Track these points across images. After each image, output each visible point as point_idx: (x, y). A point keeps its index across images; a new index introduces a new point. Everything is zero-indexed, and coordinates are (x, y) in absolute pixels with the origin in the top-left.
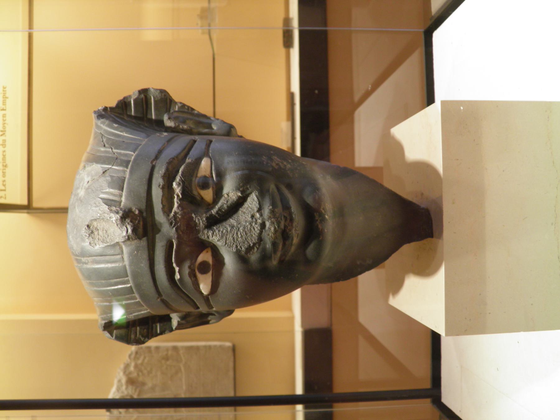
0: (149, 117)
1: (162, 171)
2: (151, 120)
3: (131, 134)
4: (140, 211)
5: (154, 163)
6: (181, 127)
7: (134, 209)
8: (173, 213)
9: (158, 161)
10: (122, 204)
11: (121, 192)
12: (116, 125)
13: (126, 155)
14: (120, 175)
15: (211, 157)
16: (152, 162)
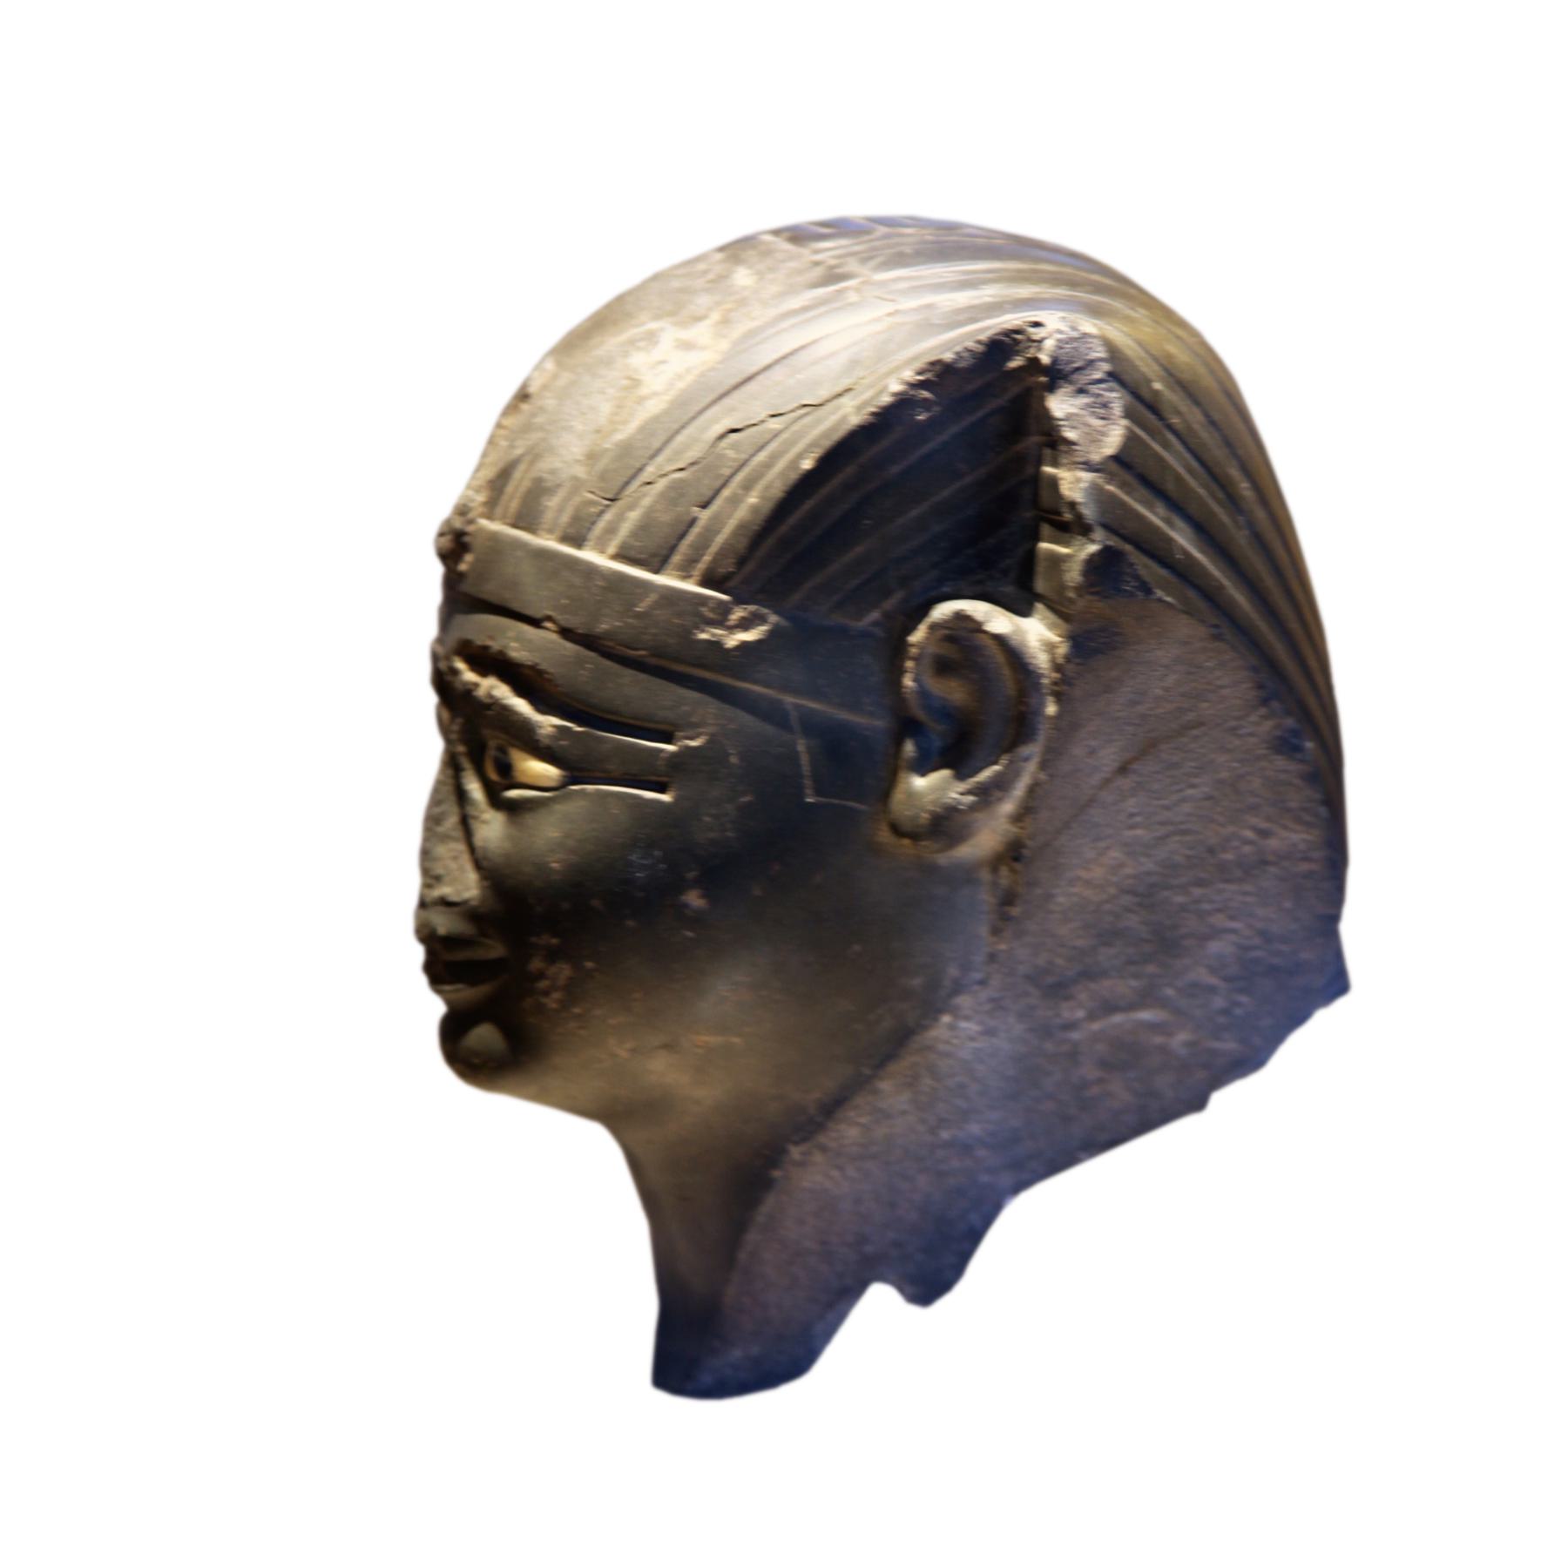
0: (1046, 529)
1: (515, 649)
2: (1036, 537)
3: (741, 527)
4: (461, 575)
5: (548, 625)
6: (909, 664)
7: (469, 558)
8: (460, 665)
9: (554, 637)
10: (484, 522)
11: (508, 521)
12: (807, 464)
13: (611, 530)
14: (549, 516)
15: (564, 791)
16: (549, 618)
